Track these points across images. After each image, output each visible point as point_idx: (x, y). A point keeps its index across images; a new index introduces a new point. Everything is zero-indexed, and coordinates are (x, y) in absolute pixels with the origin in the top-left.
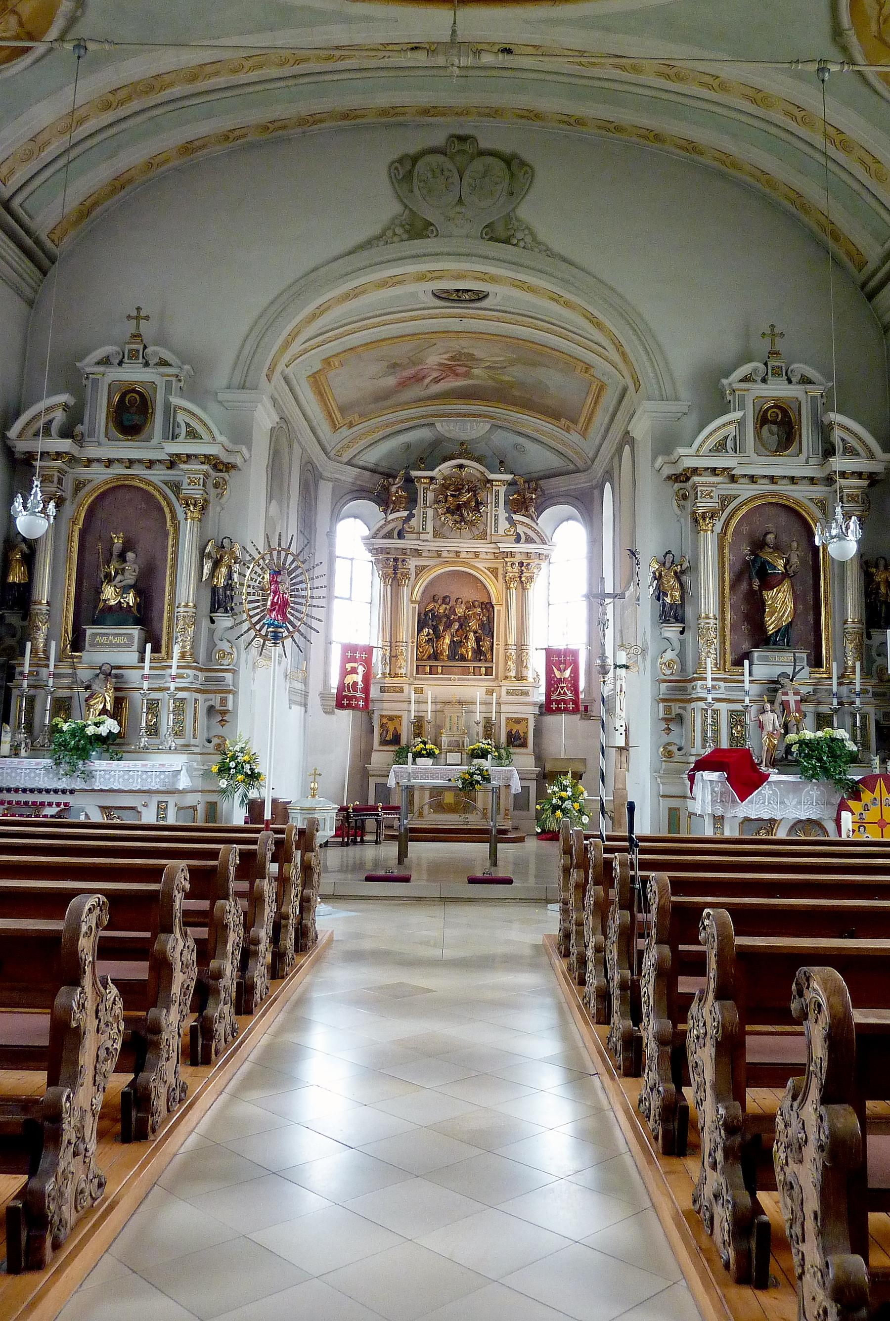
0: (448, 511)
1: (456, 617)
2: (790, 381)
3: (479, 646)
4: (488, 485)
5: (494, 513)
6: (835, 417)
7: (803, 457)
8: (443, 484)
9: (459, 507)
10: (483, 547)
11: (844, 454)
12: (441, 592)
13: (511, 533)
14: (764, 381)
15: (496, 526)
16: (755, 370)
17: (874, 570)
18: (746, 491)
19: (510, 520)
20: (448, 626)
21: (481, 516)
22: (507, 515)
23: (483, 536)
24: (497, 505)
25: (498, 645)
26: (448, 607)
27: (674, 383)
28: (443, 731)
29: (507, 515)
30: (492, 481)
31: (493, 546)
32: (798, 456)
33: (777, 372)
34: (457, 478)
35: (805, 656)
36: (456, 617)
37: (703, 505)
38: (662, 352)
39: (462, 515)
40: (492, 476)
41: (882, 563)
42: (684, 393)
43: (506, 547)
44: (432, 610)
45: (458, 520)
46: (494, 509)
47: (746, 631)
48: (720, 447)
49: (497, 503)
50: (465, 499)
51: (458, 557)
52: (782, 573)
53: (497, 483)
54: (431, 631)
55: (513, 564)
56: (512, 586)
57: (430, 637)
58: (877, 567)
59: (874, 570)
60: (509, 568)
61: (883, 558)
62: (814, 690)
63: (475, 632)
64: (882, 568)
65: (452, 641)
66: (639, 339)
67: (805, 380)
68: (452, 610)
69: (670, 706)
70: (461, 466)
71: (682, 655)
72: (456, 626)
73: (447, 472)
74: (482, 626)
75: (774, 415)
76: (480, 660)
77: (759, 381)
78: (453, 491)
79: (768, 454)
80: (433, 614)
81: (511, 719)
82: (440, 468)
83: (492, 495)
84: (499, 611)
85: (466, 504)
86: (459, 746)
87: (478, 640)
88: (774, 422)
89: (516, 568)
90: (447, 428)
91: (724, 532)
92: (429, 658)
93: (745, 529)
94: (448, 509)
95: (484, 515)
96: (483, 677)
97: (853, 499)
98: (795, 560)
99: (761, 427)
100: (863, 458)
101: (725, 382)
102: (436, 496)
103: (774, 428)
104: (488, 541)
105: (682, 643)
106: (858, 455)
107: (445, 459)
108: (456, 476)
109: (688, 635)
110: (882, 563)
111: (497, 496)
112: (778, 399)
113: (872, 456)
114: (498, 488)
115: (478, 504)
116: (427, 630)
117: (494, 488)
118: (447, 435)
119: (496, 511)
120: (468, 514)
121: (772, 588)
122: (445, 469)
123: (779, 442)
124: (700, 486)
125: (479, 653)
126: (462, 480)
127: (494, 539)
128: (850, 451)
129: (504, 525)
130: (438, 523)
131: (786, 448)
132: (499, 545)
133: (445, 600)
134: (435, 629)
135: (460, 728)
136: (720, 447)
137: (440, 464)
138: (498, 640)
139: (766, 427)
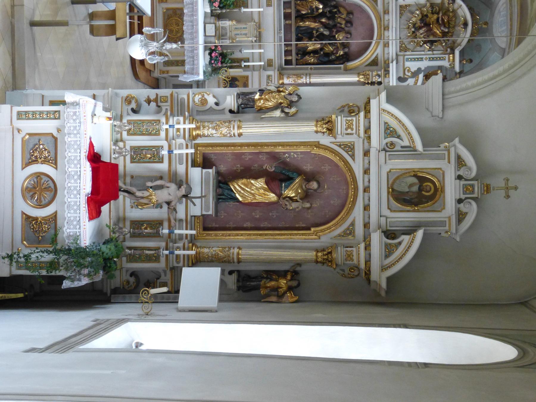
0: (424, 17)
1: (334, 34)
2: (460, 201)
3: (309, 53)
4: (449, 50)
5: (424, 57)
6: (420, 234)
7: (386, 212)
8: (448, 10)
9: (427, 25)
10: (392, 50)
11: (386, 245)
12: (357, 19)
13: (407, 73)
14: (460, 177)
15: (411, 60)
16: (470, 169)
17: (289, 277)
18: (357, 167)
19: (419, 70)
20: (325, 26)
21: (421, 46)
22: (423, 69)
23: (403, 48)
24: (431, 59)
25: (311, 69)
26: (343, 26)
27: (461, 104)
28: (234, 22)
29: (423, 69)
30: (453, 53)
31: (394, 57)
32: (389, 208)
33: (467, 189)
34: (455, 23)
35: (210, 213)
36: (334, 34)
37: (340, 122)
38: (491, 94)
39: (420, 28)
40: (457, 53)
41: (294, 283)
42: (452, 115)
43: (393, 68)
44: (340, 12)
45: (417, 26)
46: (428, 56)
47: (235, 168)
48: (389, 131)
49: (433, 59)
50: (435, 30)
51: (384, 29)
52: (281, 194)
53: (451, 58)
54: (321, 11)
55: (379, 76)
56: (361, 77)
57: (315, 10)
58: (291, 279)
59: (289, 277)
60: (375, 73)
61: (299, 285)
62: (181, 220)
63: (321, 49)
64: (290, 283)
65: (313, 29)
66: (505, 71)
67: (461, 216)
68: (340, 29)
69: (166, 102)
70: (465, 24)
71: (211, 111)
72: (326, 33)
73: (460, 12)
74: (327, 55)
75: (428, 188)
76: (297, 54)
77: (458, 173)
78: (442, 19)
79: (390, 182)
80: (336, 13)
81: (247, 80)
82: (464, 6)
83: (441, 54)
84: (340, 68)
85: (430, 31)
86: (222, 36)
87: (315, 52)
88: (420, 189)
89: (376, 79)
90: (501, 9)
91: (318, 145)
92: (298, 11)
93: (326, 168)
94: (427, 16)
95: (422, 49)
96: (284, 58)
97: (349, 256)
98: (294, 205)
99: (415, 176)
100: (381, 261)
101: (457, 140)
102: (437, 5)
103: (415, 189)
104: (399, 53)
105: (222, 111)
106: (387, 257)
107: (470, 9)
108: (457, 22)
109: (229, 116)
110: (294, 283)
111: (440, 59)
112: (443, 190)
113: (384, 268)
114: (447, 59)
115: (432, 42)
116: (321, 7)
117: (447, 56)
118: (497, 12)
119: (426, 59)
120: (421, 34)
121: (267, 183)
122: (464, 12)
123: (402, 193)
124: (356, 119)
125: (303, 52)
126: (454, 27)
127: (401, 58)
128: (389, 251)
129: (413, 66)
130: (413, 9)
131: (397, 199)
132: (395, 62)
133: (349, 22)
134: (323, 15)
135: (238, 36)
136: (389, 131)
137: (467, 6)
138: (315, 69)
139: (415, 180)
